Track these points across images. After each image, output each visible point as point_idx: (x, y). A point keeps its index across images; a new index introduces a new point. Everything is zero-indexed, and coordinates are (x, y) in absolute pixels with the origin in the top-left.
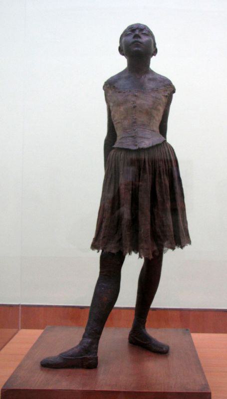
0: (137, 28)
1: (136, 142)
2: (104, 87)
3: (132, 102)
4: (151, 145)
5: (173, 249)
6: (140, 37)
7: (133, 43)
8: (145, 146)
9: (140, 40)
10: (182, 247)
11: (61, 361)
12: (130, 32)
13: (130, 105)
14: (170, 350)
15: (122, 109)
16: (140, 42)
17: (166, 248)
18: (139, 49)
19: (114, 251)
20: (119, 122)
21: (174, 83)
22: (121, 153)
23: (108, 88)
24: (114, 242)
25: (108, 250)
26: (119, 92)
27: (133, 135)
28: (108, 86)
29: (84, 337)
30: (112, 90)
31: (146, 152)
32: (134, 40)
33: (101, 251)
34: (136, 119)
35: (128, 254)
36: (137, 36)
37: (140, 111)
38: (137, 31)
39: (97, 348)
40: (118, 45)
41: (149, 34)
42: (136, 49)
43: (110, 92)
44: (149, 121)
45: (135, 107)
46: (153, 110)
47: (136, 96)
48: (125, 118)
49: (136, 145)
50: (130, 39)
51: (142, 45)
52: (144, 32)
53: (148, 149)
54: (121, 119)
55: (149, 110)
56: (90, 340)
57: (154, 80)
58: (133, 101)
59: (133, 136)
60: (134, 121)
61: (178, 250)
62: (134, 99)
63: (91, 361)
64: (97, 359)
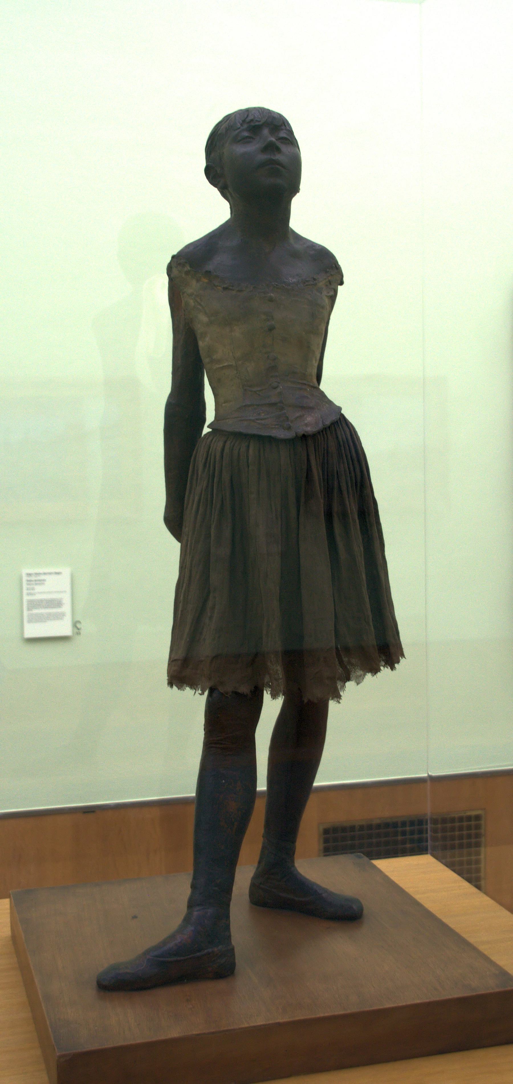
0: (266, 124)
1: (287, 419)
2: (170, 269)
4: (320, 426)
5: (375, 671)
6: (278, 150)
7: (263, 165)
8: (310, 430)
9: (278, 157)
10: (393, 668)
12: (246, 134)
14: (365, 912)
15: (238, 332)
17: (360, 673)
18: (279, 181)
19: (245, 689)
20: (229, 367)
21: (341, 262)
22: (248, 447)
23: (187, 273)
25: (229, 688)
26: (225, 289)
27: (274, 399)
28: (188, 268)
29: (191, 904)
30: (198, 281)
32: (262, 157)
33: (206, 693)
35: (252, 690)
36: (270, 148)
38: (266, 132)
39: (228, 927)
41: (291, 141)
43: (193, 286)
45: (271, 329)
47: (271, 300)
49: (289, 428)
52: (283, 134)
53: (314, 436)
56: (210, 911)
57: (296, 255)
59: (274, 404)
61: (385, 671)
64: (233, 950)
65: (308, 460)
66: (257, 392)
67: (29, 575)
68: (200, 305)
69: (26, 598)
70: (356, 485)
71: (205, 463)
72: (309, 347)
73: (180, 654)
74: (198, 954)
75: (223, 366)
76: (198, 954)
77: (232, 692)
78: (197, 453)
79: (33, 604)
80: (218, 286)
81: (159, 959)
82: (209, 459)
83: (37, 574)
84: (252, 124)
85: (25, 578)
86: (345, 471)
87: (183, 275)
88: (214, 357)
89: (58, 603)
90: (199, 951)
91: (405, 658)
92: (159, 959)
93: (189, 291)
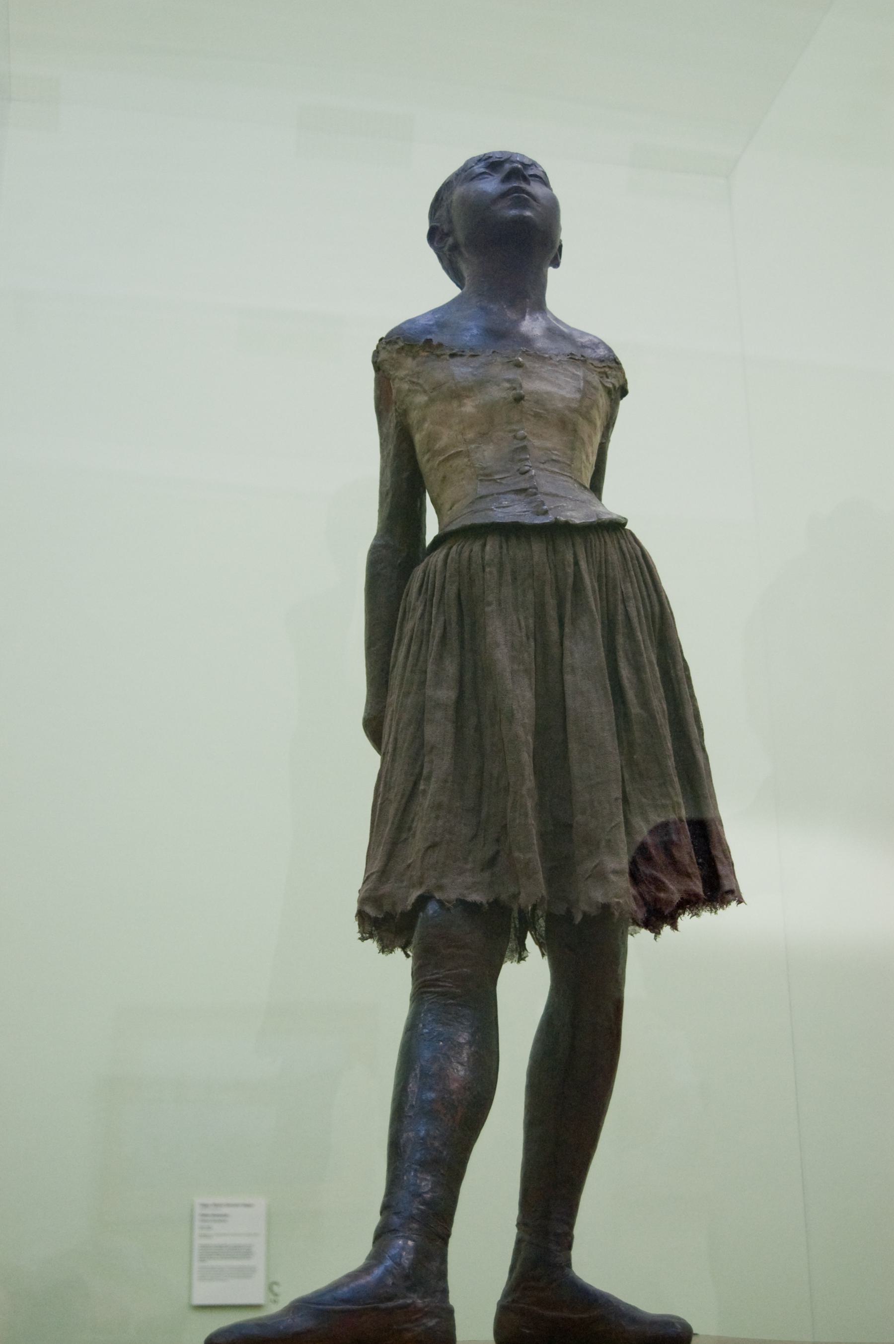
3: (507, 385)
7: (503, 195)
11: (310, 1324)
13: (497, 393)
16: (528, 193)
18: (528, 213)
22: (484, 545)
24: (469, 866)
27: (523, 485)
30: (414, 358)
31: (579, 540)
34: (524, 438)
37: (537, 415)
40: (426, 228)
42: (513, 212)
44: (569, 452)
45: (519, 399)
47: (519, 365)
48: (484, 436)
50: (491, 185)
51: (534, 203)
58: (508, 381)
60: (519, 444)
62: (512, 374)
63: (431, 1323)
65: (576, 563)
66: (498, 481)
67: (205, 1206)
68: (418, 384)
69: (198, 1242)
70: (653, 622)
71: (421, 586)
72: (575, 431)
73: (377, 866)
74: (390, 1304)
75: (449, 456)
76: (390, 1304)
77: (457, 900)
78: (410, 585)
79: (209, 1252)
80: (442, 355)
81: (317, 1307)
82: (426, 579)
83: (216, 1205)
84: (491, 160)
85: (198, 1211)
86: (634, 594)
87: (394, 355)
88: (437, 447)
89: (246, 1252)
90: (390, 1299)
91: (746, 904)
92: (317, 1307)
93: (402, 373)
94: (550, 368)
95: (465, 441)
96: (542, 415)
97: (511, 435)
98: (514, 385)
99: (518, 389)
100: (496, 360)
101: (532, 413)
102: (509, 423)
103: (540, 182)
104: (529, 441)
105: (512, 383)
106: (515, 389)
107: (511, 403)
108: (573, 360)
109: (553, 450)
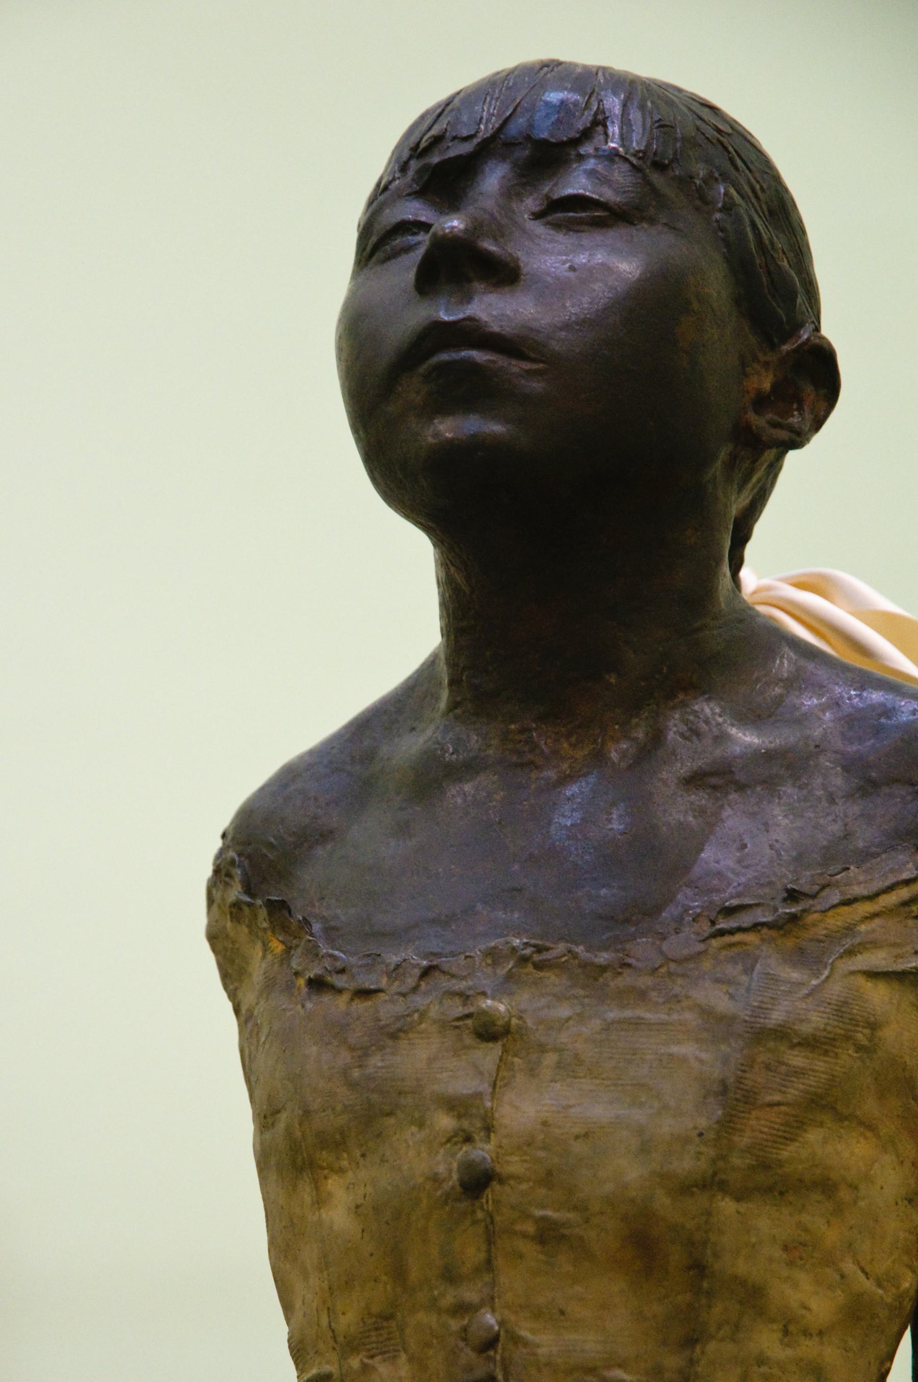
3: (445, 1122)
46: (727, 1206)
54: (350, 1346)
55: (662, 1202)
94: (613, 1015)
95: (336, 1341)
96: (566, 1232)
97: (455, 1325)
98: (465, 1124)
99: (477, 1137)
100: (423, 1015)
101: (530, 1228)
102: (450, 1276)
103: (599, 224)
104: (516, 1340)
105: (459, 1117)
106: (468, 1139)
107: (458, 1200)
108: (728, 939)
109: (609, 1367)
